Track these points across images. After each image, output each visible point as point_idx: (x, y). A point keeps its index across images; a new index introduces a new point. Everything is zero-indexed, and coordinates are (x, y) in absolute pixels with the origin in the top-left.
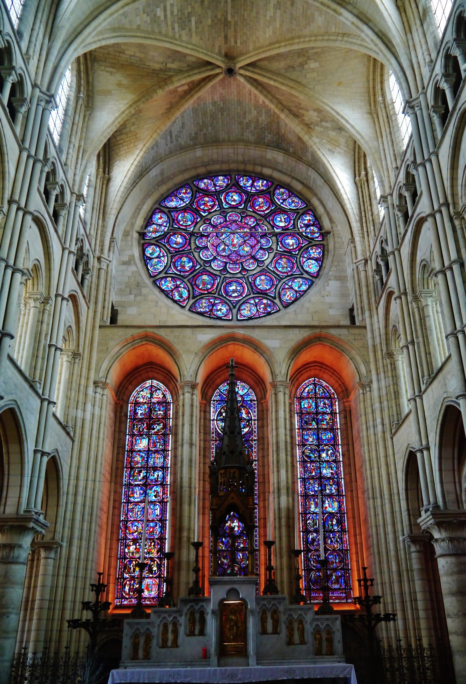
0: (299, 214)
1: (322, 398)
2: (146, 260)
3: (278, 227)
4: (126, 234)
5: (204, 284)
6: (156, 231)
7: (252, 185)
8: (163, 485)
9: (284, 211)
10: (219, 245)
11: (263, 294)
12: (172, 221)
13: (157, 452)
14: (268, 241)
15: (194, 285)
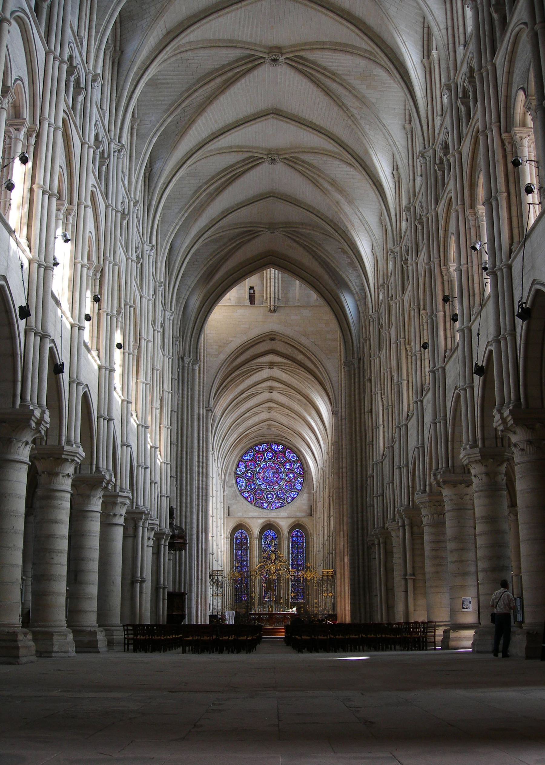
0: (294, 462)
1: (300, 537)
2: (237, 484)
3: (287, 469)
4: (230, 474)
5: (259, 494)
6: (240, 471)
7: (277, 448)
8: (247, 566)
9: (289, 461)
10: (264, 478)
11: (280, 497)
12: (247, 466)
13: (244, 555)
14: (283, 475)
15: (256, 495)
